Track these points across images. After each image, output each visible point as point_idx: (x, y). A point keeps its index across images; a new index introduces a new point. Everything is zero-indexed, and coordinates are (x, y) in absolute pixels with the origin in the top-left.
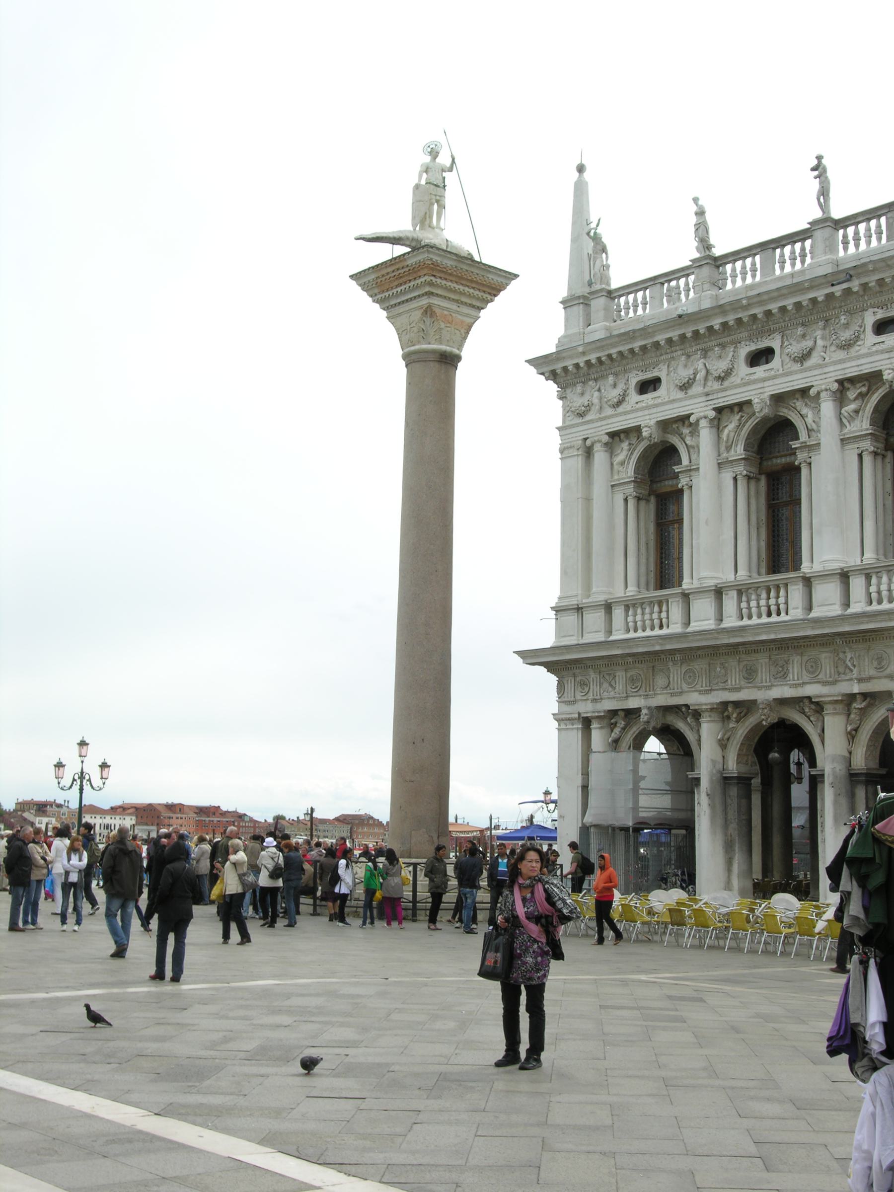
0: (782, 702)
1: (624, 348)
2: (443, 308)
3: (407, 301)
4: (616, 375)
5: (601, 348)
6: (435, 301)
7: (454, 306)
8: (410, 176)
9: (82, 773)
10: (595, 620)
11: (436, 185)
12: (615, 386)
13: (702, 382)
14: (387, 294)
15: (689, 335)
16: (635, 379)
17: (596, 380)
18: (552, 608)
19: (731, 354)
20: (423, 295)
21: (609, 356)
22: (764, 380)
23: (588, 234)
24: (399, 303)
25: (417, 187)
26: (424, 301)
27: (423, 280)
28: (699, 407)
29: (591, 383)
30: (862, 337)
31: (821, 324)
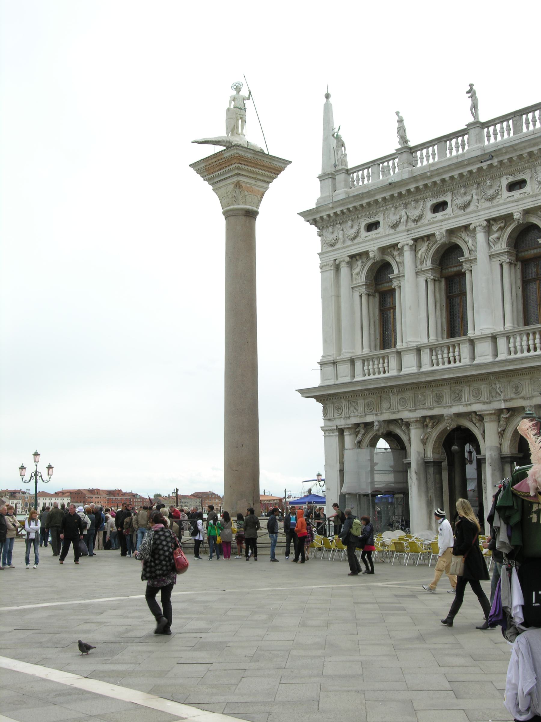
0: (459, 415)
1: (357, 204)
2: (246, 183)
4: (353, 220)
5: (343, 205)
6: (241, 179)
7: (253, 182)
8: (225, 103)
9: (36, 472)
10: (344, 369)
12: (352, 227)
13: (405, 223)
14: (212, 175)
15: (396, 195)
16: (364, 222)
17: (340, 224)
18: (318, 363)
19: (422, 206)
20: (234, 175)
21: (348, 209)
22: (442, 221)
23: (333, 135)
24: (220, 181)
25: (228, 110)
26: (235, 179)
27: (234, 166)
28: (403, 238)
29: (337, 226)
30: (500, 193)
31: (475, 186)
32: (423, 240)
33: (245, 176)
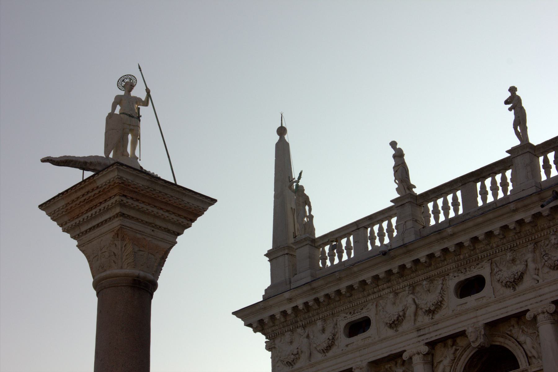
3: (98, 226)
4: (324, 320)
6: (128, 223)
7: (148, 230)
11: (130, 116)
13: (413, 318)
14: (77, 221)
16: (343, 322)
17: (304, 327)
19: (440, 287)
20: (114, 217)
22: (476, 309)
23: (290, 187)
24: (90, 229)
25: (111, 117)
27: (113, 200)
29: (299, 330)
31: (531, 247)
32: (445, 346)
33: (132, 218)
